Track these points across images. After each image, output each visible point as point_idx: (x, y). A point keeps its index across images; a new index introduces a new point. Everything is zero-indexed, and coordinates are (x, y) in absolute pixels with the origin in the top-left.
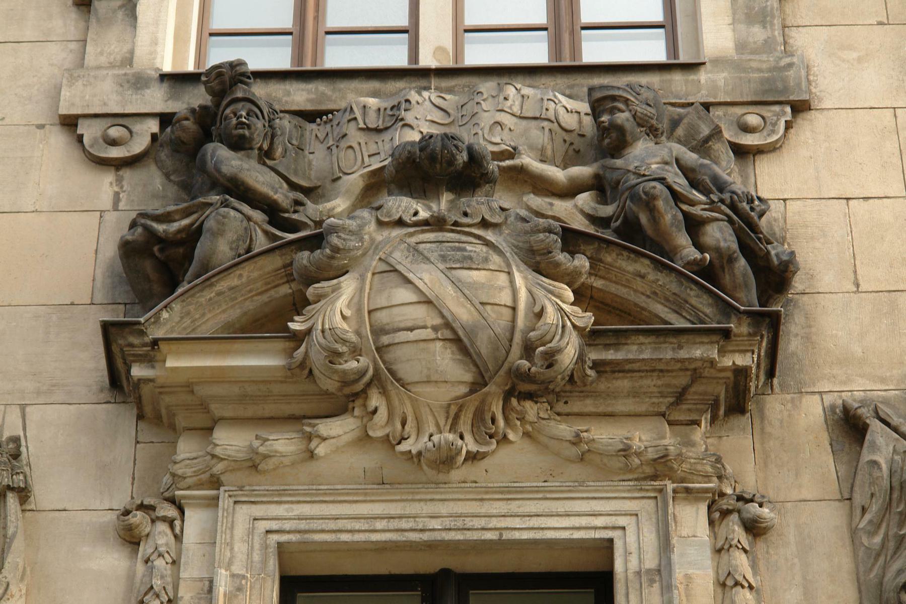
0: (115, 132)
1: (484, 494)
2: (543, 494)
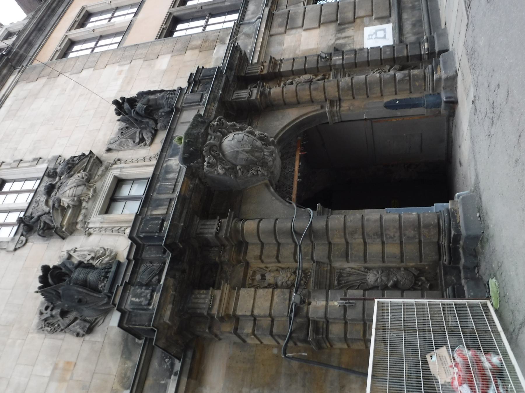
0: (20, 242)
1: (101, 189)
2: (104, 182)
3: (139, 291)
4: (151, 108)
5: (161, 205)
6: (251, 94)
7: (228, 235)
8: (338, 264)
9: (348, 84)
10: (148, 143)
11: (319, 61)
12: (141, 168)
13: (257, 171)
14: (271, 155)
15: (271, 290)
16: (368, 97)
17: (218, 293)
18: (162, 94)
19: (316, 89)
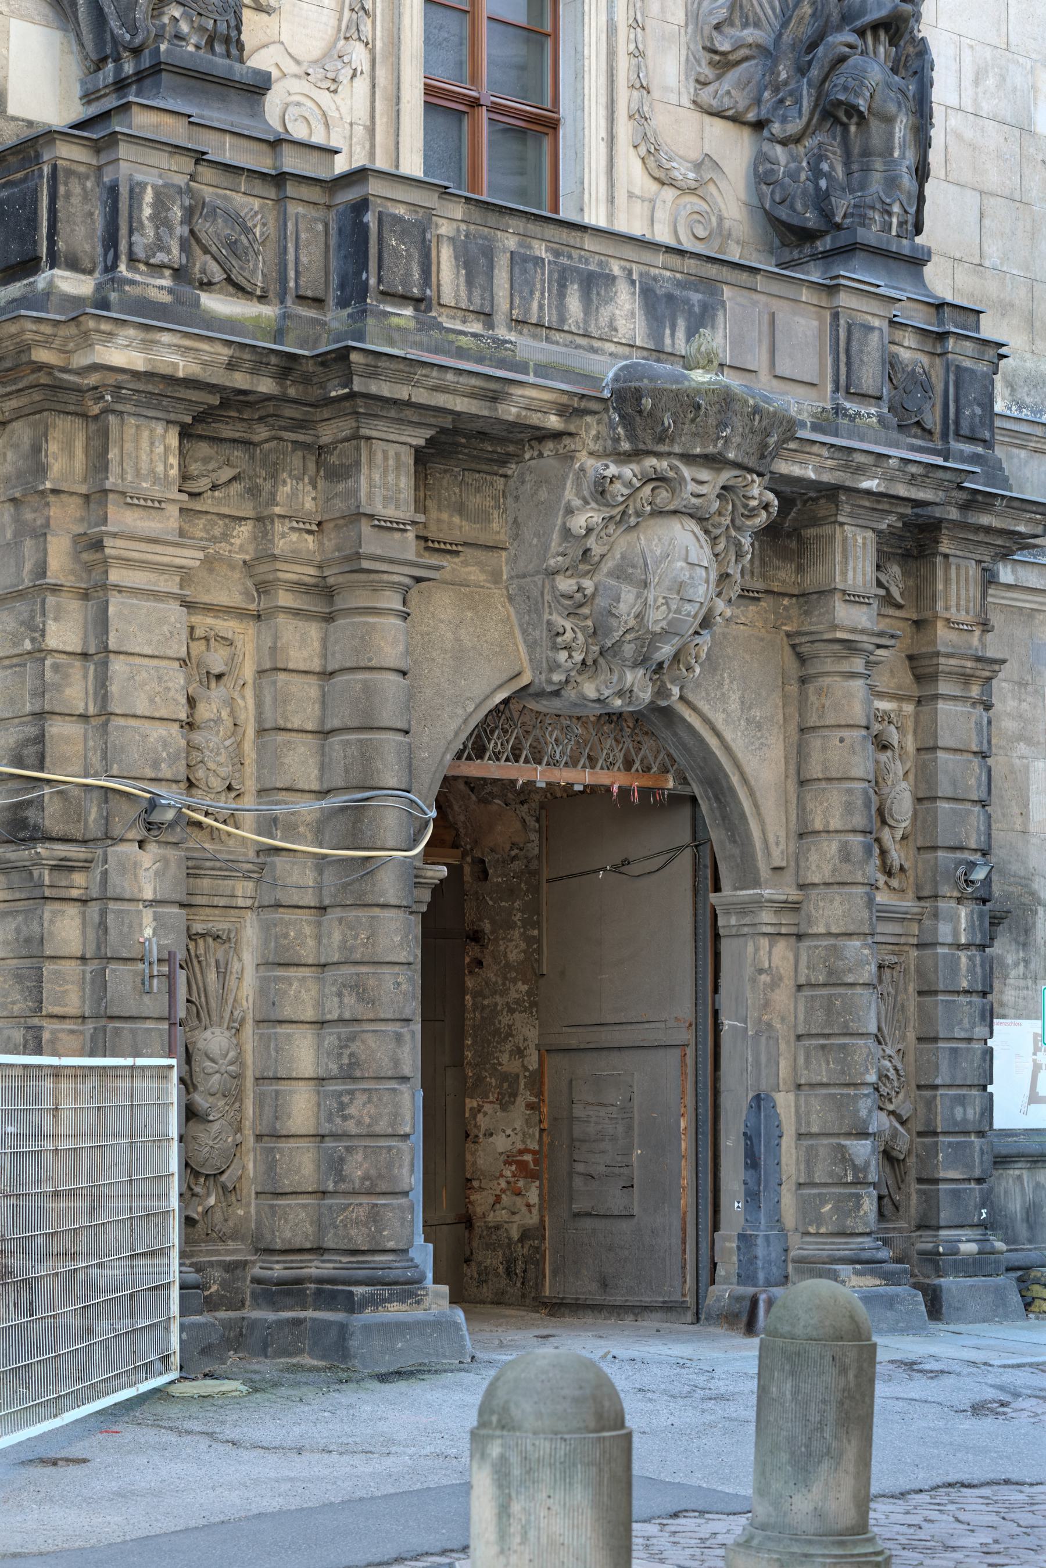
3: (177, 213)
4: (853, 129)
5: (470, 282)
6: (854, 599)
7: (366, 564)
8: (250, 932)
9: (850, 971)
10: (706, 96)
11: (959, 855)
12: (603, 80)
13: (568, 648)
14: (620, 694)
15: (183, 716)
16: (799, 1037)
17: (169, 521)
18: (908, 182)
19: (845, 856)
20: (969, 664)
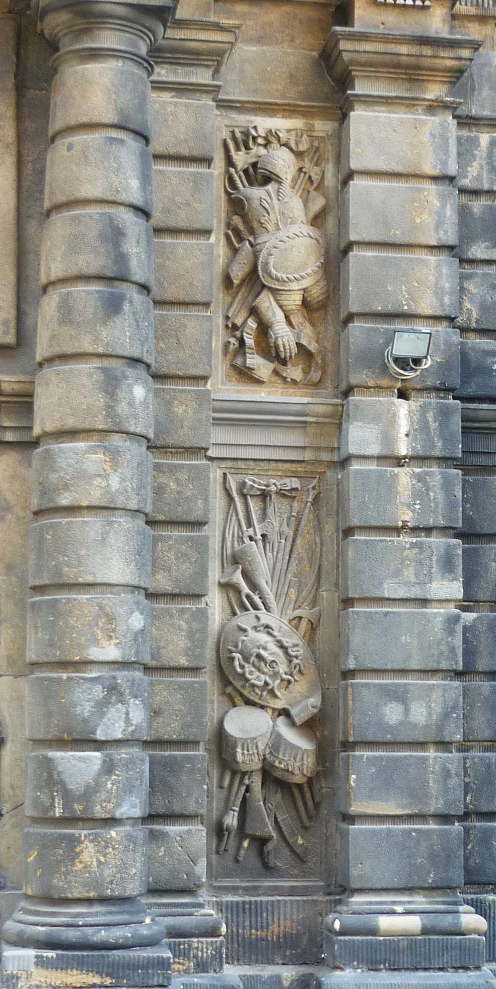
20: (404, 49)
